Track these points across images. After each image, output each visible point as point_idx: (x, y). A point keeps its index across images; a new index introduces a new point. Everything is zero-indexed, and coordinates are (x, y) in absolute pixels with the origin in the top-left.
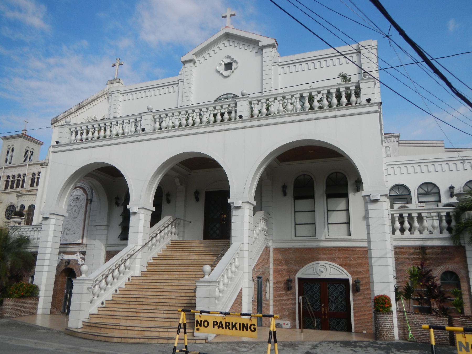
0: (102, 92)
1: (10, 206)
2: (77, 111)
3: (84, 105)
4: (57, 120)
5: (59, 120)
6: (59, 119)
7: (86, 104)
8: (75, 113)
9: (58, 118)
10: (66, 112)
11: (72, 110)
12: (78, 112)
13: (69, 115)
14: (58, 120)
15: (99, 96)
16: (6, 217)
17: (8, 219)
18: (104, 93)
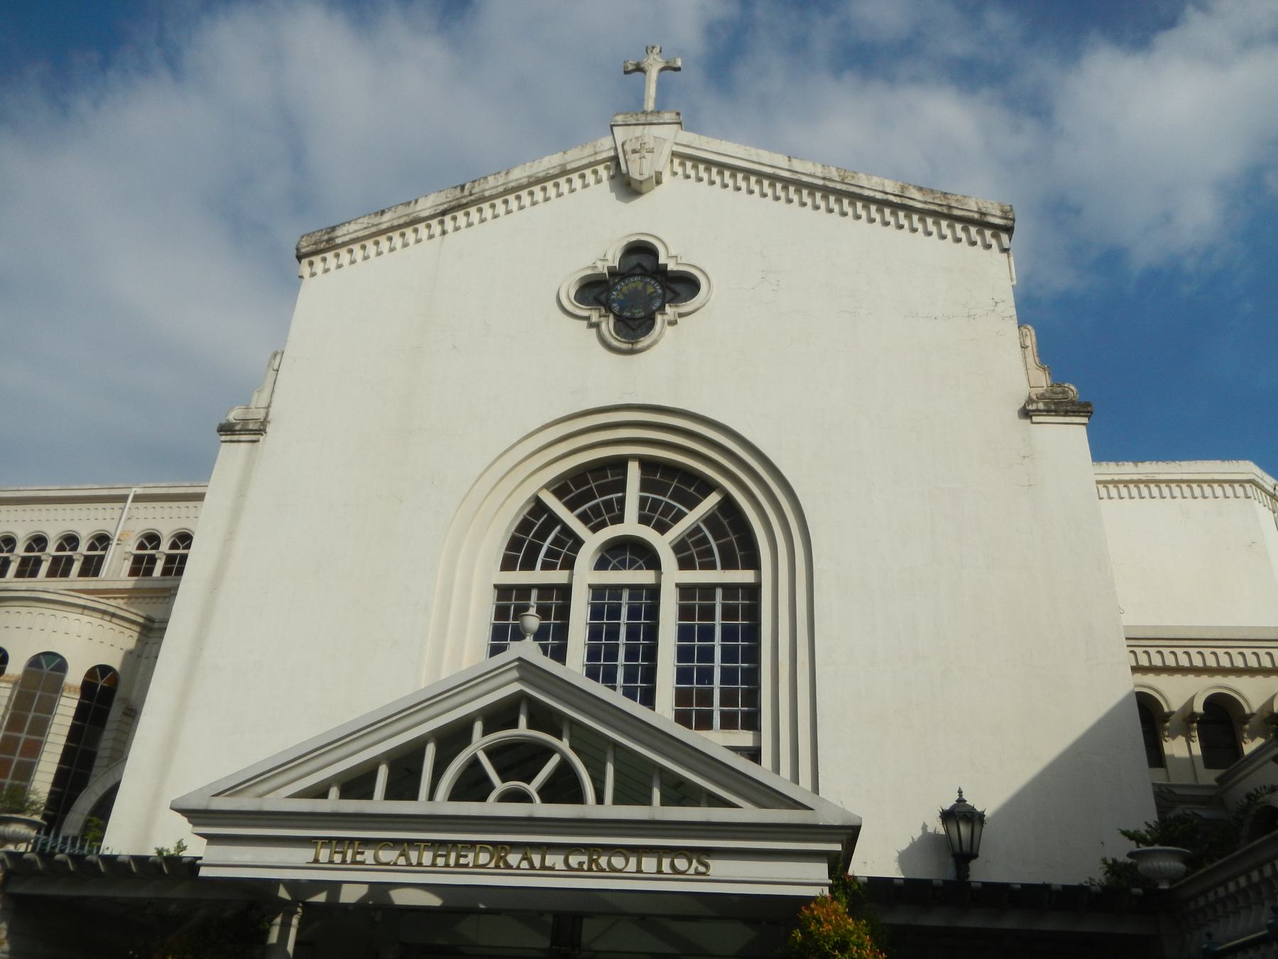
0: (588, 150)
2: (444, 213)
3: (487, 194)
4: (332, 239)
5: (344, 244)
6: (347, 238)
7: (501, 189)
8: (434, 222)
9: (339, 232)
10: (383, 212)
11: (420, 206)
12: (447, 218)
13: (400, 227)
14: (339, 241)
15: (569, 167)
18: (599, 157)
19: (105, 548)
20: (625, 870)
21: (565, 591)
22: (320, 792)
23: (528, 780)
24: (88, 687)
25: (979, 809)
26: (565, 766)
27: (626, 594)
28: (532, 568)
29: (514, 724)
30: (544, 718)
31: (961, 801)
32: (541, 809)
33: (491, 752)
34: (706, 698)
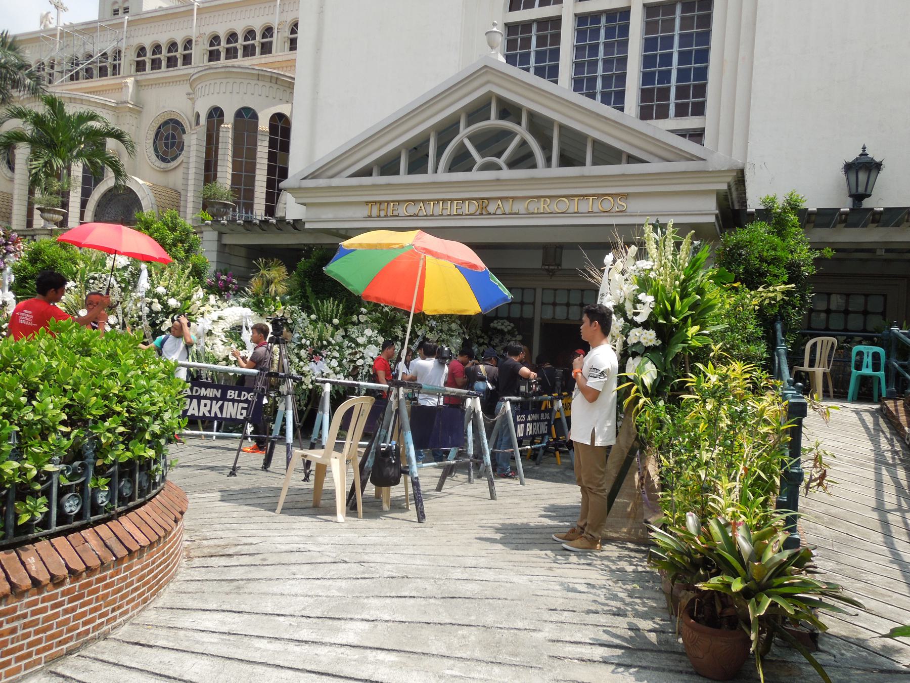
1: (166, 123)
16: (158, 156)
17: (164, 160)
19: (272, 36)
20: (568, 211)
21: (556, 21)
22: (366, 172)
23: (499, 155)
24: (273, 128)
25: (877, 160)
26: (524, 143)
27: (603, 20)
28: (532, 6)
29: (489, 118)
30: (509, 110)
31: (864, 154)
32: (506, 173)
33: (471, 138)
34: (664, 94)
